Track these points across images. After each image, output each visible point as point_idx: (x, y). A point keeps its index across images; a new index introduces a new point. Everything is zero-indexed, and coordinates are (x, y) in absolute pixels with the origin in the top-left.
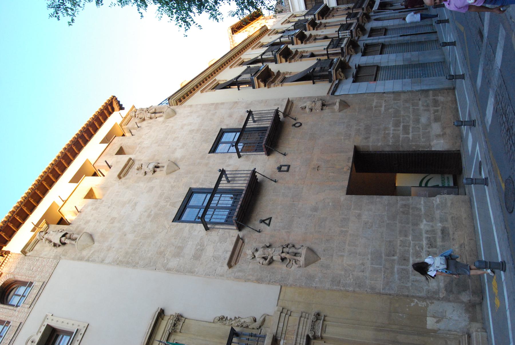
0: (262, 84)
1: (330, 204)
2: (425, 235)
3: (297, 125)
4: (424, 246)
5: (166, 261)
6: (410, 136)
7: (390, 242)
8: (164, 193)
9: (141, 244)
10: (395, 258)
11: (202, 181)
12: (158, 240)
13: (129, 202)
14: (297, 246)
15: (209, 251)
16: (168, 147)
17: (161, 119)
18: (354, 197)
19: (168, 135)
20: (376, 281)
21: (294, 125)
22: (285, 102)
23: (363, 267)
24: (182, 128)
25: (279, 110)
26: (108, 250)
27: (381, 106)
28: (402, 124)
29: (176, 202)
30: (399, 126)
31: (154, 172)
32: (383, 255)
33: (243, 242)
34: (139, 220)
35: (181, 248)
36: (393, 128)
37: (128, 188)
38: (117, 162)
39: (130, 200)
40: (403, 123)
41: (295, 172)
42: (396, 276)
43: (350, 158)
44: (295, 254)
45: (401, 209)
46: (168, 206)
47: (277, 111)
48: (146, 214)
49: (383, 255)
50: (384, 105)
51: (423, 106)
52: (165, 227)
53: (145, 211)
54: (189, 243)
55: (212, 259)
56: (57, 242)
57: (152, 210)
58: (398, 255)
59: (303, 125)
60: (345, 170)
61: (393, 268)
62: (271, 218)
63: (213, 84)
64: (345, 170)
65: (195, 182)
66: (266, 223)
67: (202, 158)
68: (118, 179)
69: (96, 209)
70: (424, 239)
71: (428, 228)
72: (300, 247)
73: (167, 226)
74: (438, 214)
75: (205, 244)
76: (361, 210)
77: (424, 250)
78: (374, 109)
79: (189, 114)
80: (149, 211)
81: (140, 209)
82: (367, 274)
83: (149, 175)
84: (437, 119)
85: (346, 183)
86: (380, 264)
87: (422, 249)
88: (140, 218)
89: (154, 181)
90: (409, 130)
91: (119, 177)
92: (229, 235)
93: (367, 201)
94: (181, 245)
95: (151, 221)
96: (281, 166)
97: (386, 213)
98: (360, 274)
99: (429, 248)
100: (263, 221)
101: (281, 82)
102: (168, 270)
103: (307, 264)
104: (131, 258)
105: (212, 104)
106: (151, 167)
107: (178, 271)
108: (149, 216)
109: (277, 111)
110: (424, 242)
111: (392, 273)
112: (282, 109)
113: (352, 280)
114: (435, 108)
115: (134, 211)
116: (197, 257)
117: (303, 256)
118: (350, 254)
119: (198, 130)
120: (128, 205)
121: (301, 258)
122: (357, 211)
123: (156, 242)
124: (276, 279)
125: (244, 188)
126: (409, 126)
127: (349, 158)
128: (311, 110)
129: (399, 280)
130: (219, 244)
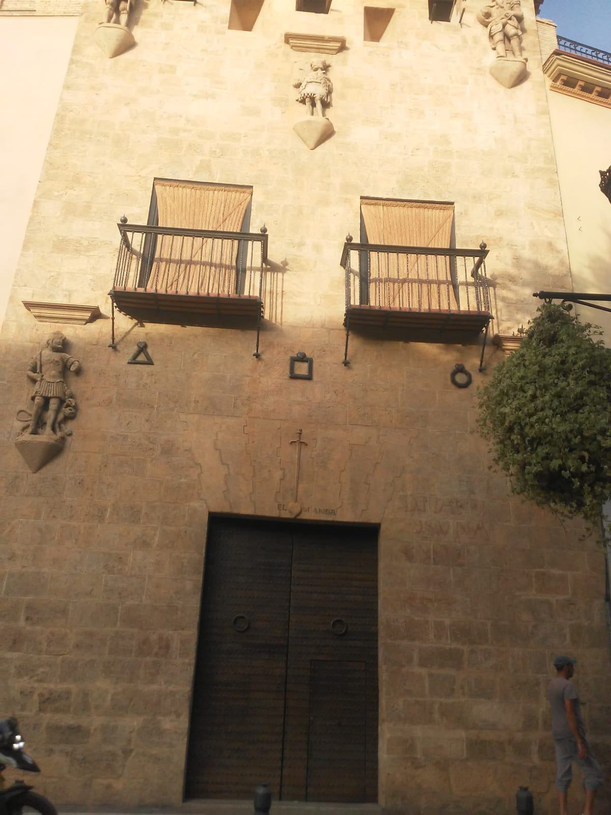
1: (183, 480)
4: (45, 685)
6: (417, 670)
7: (64, 612)
10: (22, 623)
14: (70, 426)
17: (490, 59)
21: (460, 369)
28: (466, 648)
31: (303, 101)
32: (30, 598)
36: (447, 622)
45: (154, 637)
49: (30, 598)
53: (188, 121)
55: (52, 274)
58: (29, 628)
59: (462, 392)
62: (152, 364)
74: (132, 722)
75: (91, 253)
77: (36, 685)
83: (296, 94)
84: (479, 749)
87: (40, 681)
91: (288, 38)
96: (310, 362)
99: (41, 695)
102: (36, 204)
114: (535, 748)
116: (62, 246)
118: (40, 530)
122: (157, 539)
123: (103, 164)
127: (333, 512)
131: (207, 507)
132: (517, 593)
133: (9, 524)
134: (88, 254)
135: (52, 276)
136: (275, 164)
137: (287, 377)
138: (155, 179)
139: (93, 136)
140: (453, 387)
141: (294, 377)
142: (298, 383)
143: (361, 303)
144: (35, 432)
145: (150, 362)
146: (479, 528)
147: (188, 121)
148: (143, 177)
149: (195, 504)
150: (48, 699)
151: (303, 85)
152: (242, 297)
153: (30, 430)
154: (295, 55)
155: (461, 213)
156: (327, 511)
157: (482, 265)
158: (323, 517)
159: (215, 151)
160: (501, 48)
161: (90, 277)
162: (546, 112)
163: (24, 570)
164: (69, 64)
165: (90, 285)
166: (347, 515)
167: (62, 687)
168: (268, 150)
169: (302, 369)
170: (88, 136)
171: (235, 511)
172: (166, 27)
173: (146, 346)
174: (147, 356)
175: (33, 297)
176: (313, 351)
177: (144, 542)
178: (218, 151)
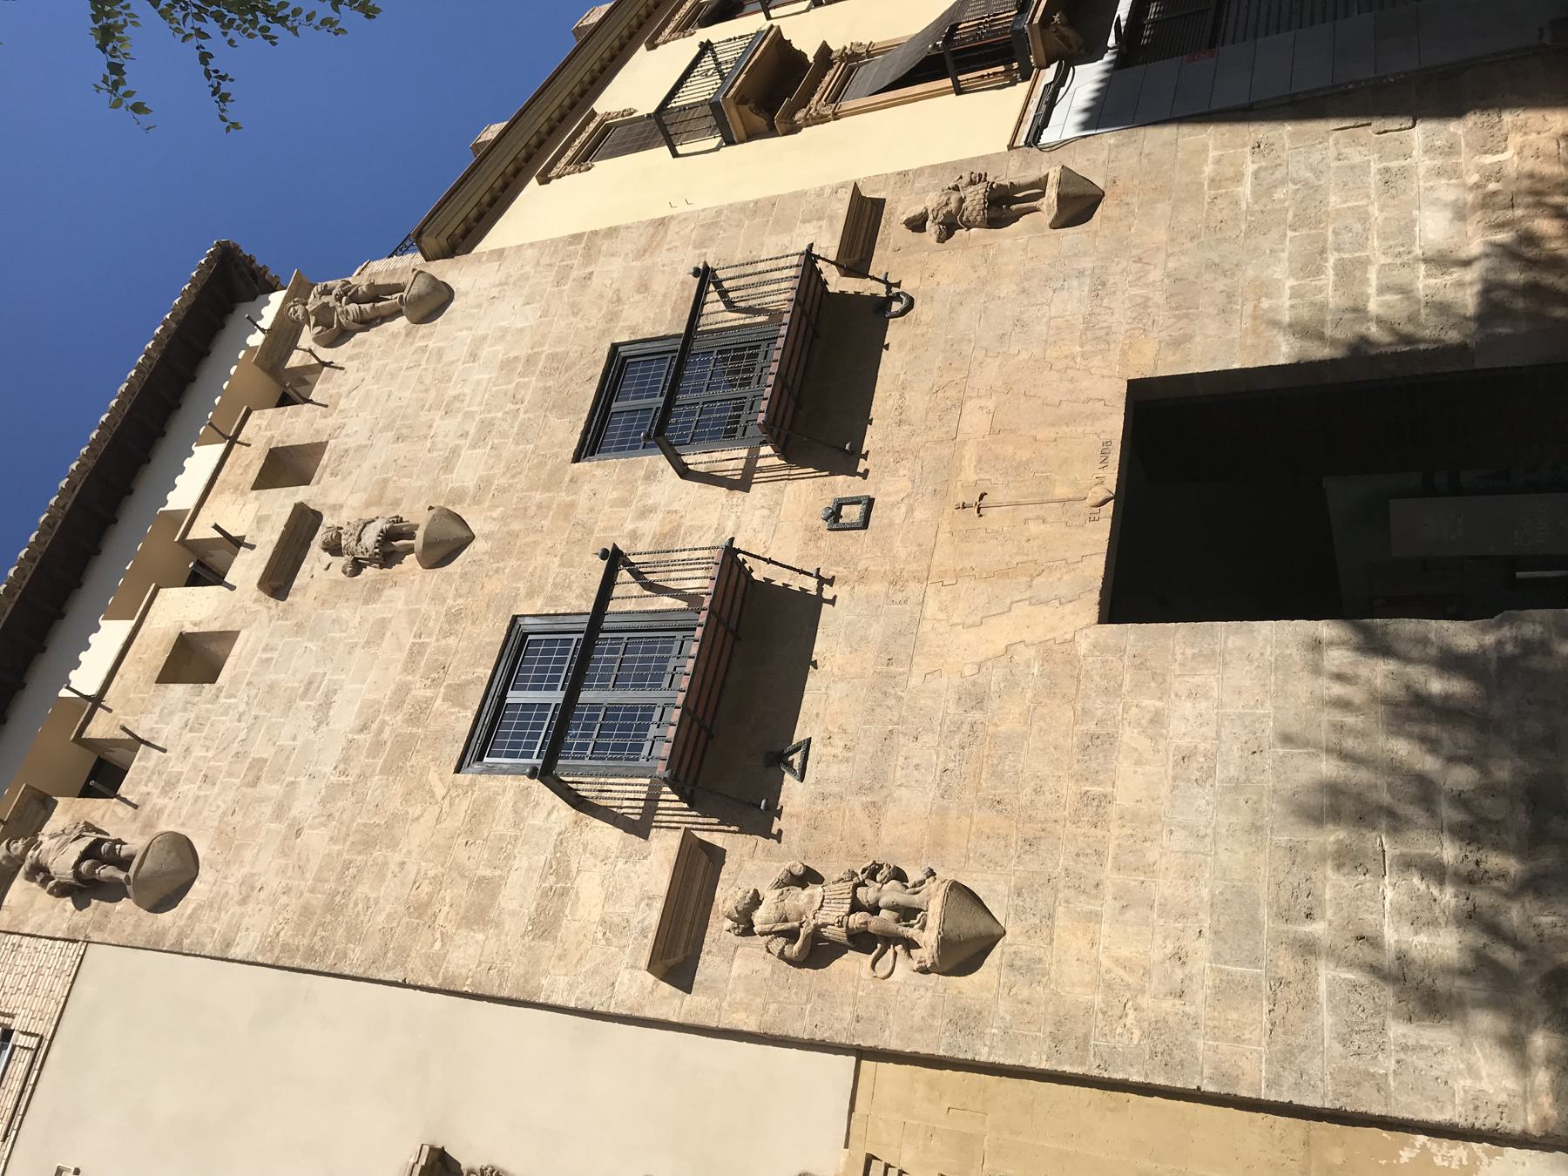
5: (438, 945)
9: (353, 871)
11: (555, 585)
13: (307, 689)
14: (914, 875)
16: (428, 444)
18: (1131, 635)
20: (1238, 1039)
22: (841, 209)
23: (1179, 973)
24: (473, 356)
25: (815, 251)
26: (244, 901)
27: (1238, 178)
28: (1332, 258)
29: (469, 683)
30: (1319, 271)
32: (1264, 913)
34: (341, 767)
35: (488, 888)
36: (1291, 282)
37: (299, 628)
39: (310, 683)
40: (1338, 249)
41: (891, 524)
42: (1327, 1019)
43: (1108, 443)
44: (907, 913)
46: (439, 702)
47: (810, 258)
48: (365, 739)
49: (1264, 913)
50: (1250, 168)
51: (1429, 150)
52: (433, 796)
53: (363, 728)
54: (516, 864)
55: (600, 935)
58: (1329, 914)
59: (917, 304)
61: (1307, 977)
65: (531, 594)
72: (921, 877)
73: (440, 791)
75: (574, 870)
76: (1163, 694)
78: (1208, 193)
79: (495, 292)
80: (375, 726)
81: (344, 718)
82: (1198, 1004)
85: (1095, 567)
86: (1255, 962)
88: (346, 760)
90: (1365, 281)
93: (1189, 652)
94: (488, 873)
95: (386, 770)
96: (840, 504)
97: (1268, 709)
98: (1168, 1005)
104: (321, 933)
105: (576, 238)
108: (378, 745)
109: (810, 258)
111: (1308, 1003)
112: (828, 244)
113: (1137, 1033)
114: (1489, 159)
115: (324, 728)
119: (530, 361)
122: (1146, 702)
123: (403, 864)
124: (837, 1026)
126: (1365, 263)
129: (1344, 1041)
130: (620, 864)
131: (1088, 626)
132: (1244, 206)
133: (1108, 971)
141: (865, 524)
146: (1140, 260)
147: (363, 728)
149: (1083, 646)
156: (1105, 454)
158: (1115, 457)
161: (620, 864)
163: (1206, 933)
165: (635, 864)
166: (1115, 425)
169: (852, 513)
170: (338, 898)
171: (1099, 583)
177: (1152, 721)
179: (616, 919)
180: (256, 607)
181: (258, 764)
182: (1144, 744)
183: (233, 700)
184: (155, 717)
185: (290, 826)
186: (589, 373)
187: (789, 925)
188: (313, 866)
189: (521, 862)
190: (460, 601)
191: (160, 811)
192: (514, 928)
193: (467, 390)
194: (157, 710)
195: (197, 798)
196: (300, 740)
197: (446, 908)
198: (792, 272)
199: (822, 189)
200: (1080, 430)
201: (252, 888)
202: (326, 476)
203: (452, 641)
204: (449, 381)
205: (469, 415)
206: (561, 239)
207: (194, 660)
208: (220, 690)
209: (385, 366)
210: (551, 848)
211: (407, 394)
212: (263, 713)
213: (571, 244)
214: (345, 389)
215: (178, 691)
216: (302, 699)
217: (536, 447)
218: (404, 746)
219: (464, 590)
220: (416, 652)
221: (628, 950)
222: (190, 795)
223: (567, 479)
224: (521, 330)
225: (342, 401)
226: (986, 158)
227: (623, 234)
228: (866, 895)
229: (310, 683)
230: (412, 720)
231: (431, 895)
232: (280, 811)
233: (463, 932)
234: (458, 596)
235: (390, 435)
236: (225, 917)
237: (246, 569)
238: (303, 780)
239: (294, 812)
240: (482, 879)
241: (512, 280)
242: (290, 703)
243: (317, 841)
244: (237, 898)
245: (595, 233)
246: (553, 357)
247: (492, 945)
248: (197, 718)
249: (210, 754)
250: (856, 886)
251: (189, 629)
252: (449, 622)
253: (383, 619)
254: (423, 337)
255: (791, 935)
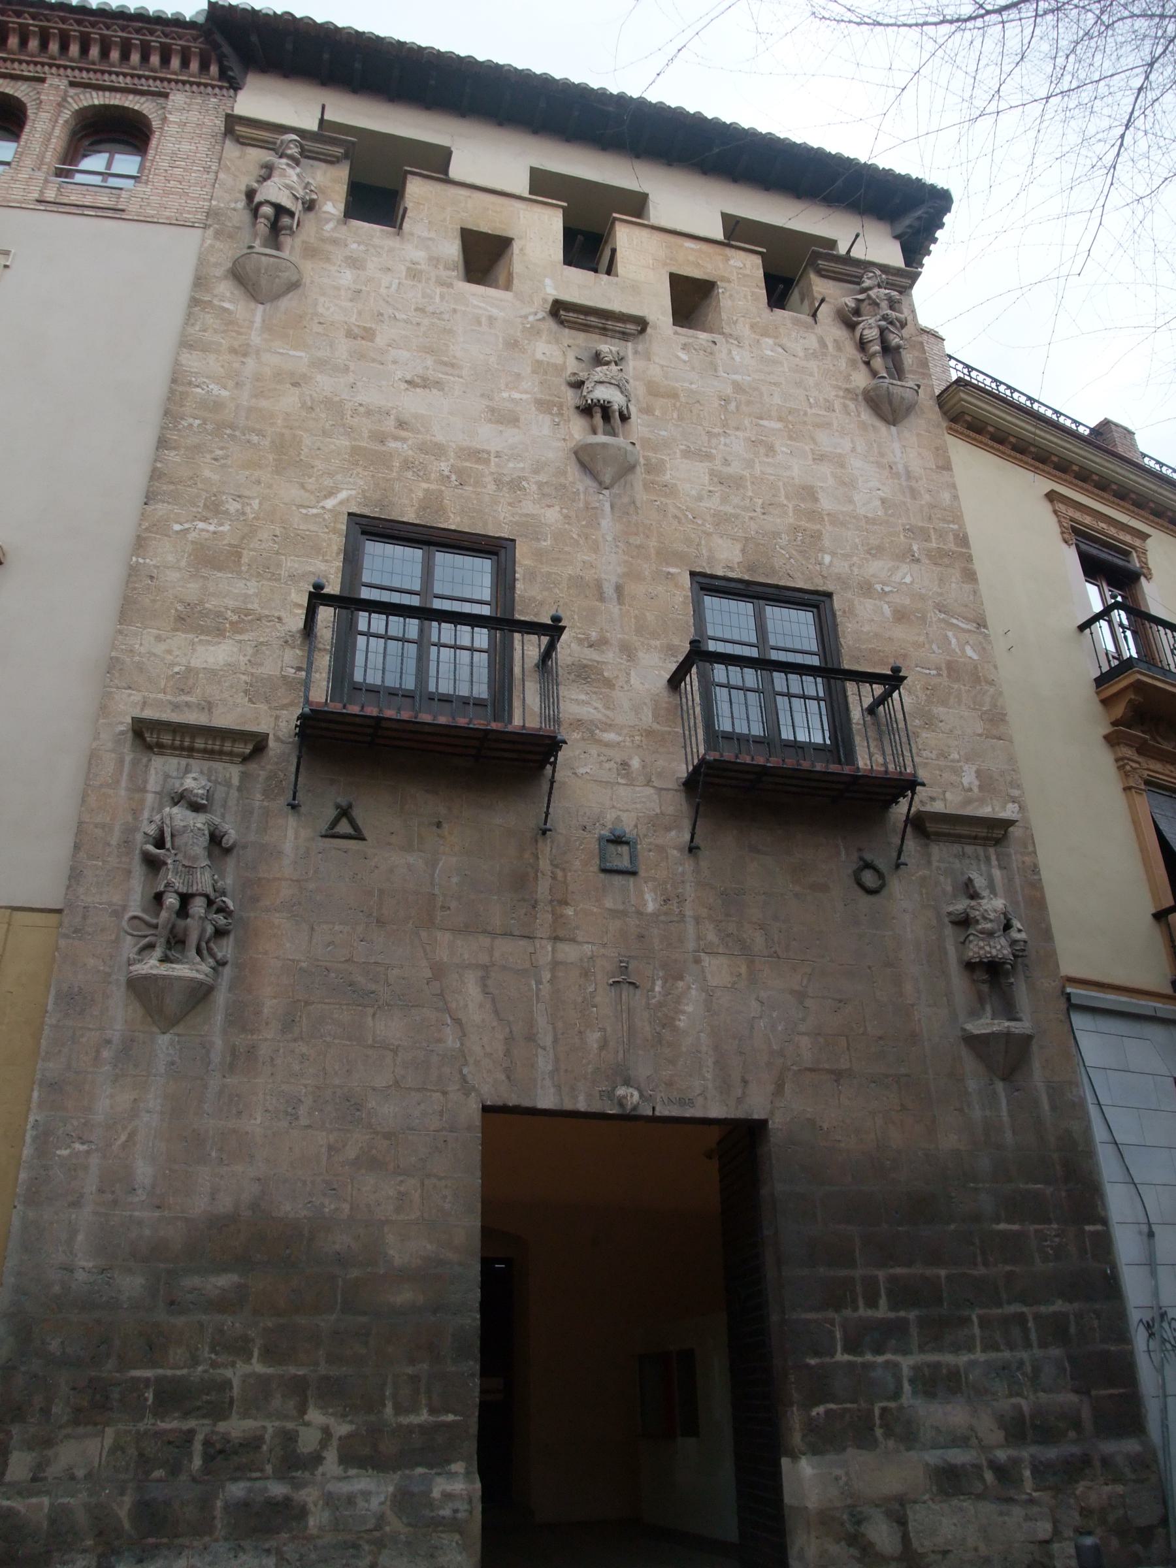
0: (1119, 710)
2: (271, 1426)
3: (869, 878)
5: (177, 527)
8: (487, 462)
9: (255, 439)
12: (270, 487)
14: (226, 949)
15: (217, 654)
19: (780, 419)
21: (868, 866)
24: (820, 458)
26: (233, 351)
31: (586, 410)
33: (245, 759)
37: (513, 345)
38: (635, 288)
39: (453, 365)
46: (425, 485)
48: (389, 425)
52: (326, 497)
53: (401, 424)
55: (176, 669)
56: (258, 198)
57: (404, 440)
59: (873, 899)
60: (621, 1091)
62: (364, 839)
63: (1112, 531)
64: (621, 1091)
66: (335, 823)
67: (666, 555)
68: (548, 306)
69: (414, 274)
70: (250, 1424)
71: (308, 1441)
72: (220, 955)
73: (330, 503)
75: (245, 637)
81: (413, 403)
85: (546, 1100)
88: (369, 413)
89: (546, 420)
92: (284, 707)
94: (245, 560)
95: (355, 450)
99: (207, 1443)
100: (344, 813)
101: (1147, 783)
102: (140, 544)
103: (142, 989)
104: (198, 422)
106: (602, 393)
107: (133, 572)
110: (236, 1427)
115: (404, 386)
117: (163, 970)
119: (814, 515)
120: (429, 362)
121: (153, 962)
125: (517, 721)
128: (964, 922)
130: (244, 677)
134: (238, 637)
135: (177, 673)
136: (549, 506)
137: (596, 869)
138: (349, 514)
139: (237, 433)
140: (860, 892)
142: (618, 880)
143: (707, 750)
144: (165, 959)
145: (359, 836)
148: (330, 511)
150: (221, 1452)
151: (588, 385)
152: (510, 729)
153: (158, 953)
154: (567, 336)
155: (844, 612)
156: (682, 1102)
157: (896, 695)
159: (448, 477)
160: (878, 363)
162: (947, 467)
164: (190, 307)
167: (250, 1424)
168: (536, 483)
170: (228, 431)
172: (354, 263)
173: (350, 806)
174: (352, 823)
175: (142, 709)
176: (636, 826)
178: (454, 477)
179: (191, 682)
180: (537, 301)
181: (368, 334)
182: (351, 1153)
183: (437, 300)
184: (425, 234)
185: (304, 376)
186: (797, 575)
187: (168, 839)
188: (264, 403)
189: (252, 587)
190: (534, 487)
191: (328, 260)
192: (192, 590)
193: (780, 457)
194: (433, 235)
195: (338, 289)
196: (392, 367)
197: (212, 528)
198: (891, 767)
199: (1019, 787)
200: (709, 1076)
201: (245, 355)
202: (683, 340)
203: (491, 487)
204: (790, 438)
205: (750, 464)
206: (962, 526)
207: (484, 256)
208: (450, 285)
209: (811, 375)
210: (267, 612)
211: (777, 400)
212: (423, 329)
213: (956, 536)
214: (784, 341)
215: (452, 249)
216: (435, 361)
217: (709, 534)
218: (381, 460)
219: (546, 490)
220: (477, 455)
221: (161, 696)
222: (342, 282)
223: (672, 570)
224: (851, 501)
225: (770, 341)
226: (1051, 957)
227: (967, 587)
228: (198, 907)
229: (453, 365)
230: (407, 465)
231: (226, 512)
232: (320, 364)
233: (189, 548)
234: (540, 485)
235: (729, 390)
236: (217, 338)
237: (582, 286)
238: (351, 378)
239: (319, 378)
240: (240, 556)
241: (913, 483)
242: (430, 351)
243: (290, 401)
244: (236, 344)
245: (969, 559)
246: (817, 536)
247: (173, 576)
248: (421, 272)
249: (383, 291)
250: (207, 896)
251: (516, 247)
252: (512, 481)
253: (517, 420)
254: (845, 406)
255: (160, 843)
